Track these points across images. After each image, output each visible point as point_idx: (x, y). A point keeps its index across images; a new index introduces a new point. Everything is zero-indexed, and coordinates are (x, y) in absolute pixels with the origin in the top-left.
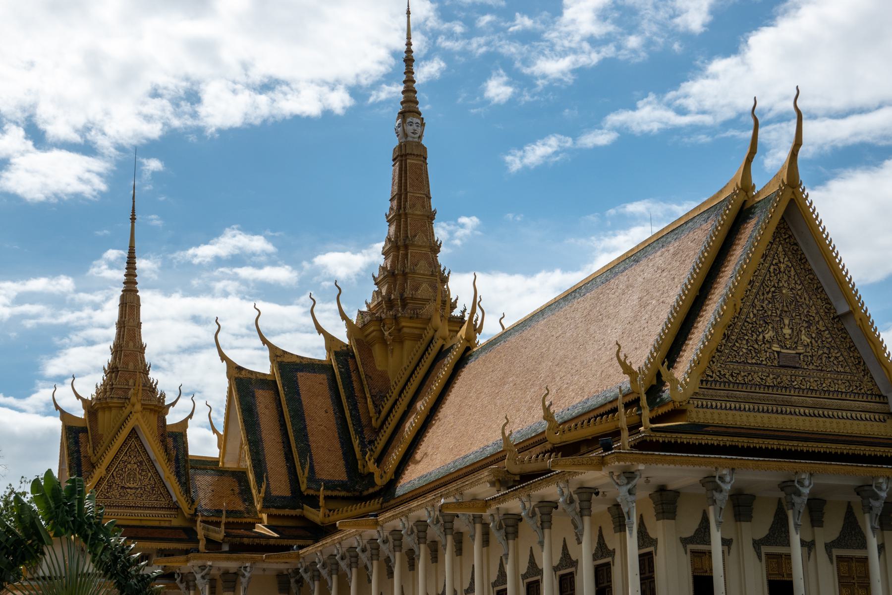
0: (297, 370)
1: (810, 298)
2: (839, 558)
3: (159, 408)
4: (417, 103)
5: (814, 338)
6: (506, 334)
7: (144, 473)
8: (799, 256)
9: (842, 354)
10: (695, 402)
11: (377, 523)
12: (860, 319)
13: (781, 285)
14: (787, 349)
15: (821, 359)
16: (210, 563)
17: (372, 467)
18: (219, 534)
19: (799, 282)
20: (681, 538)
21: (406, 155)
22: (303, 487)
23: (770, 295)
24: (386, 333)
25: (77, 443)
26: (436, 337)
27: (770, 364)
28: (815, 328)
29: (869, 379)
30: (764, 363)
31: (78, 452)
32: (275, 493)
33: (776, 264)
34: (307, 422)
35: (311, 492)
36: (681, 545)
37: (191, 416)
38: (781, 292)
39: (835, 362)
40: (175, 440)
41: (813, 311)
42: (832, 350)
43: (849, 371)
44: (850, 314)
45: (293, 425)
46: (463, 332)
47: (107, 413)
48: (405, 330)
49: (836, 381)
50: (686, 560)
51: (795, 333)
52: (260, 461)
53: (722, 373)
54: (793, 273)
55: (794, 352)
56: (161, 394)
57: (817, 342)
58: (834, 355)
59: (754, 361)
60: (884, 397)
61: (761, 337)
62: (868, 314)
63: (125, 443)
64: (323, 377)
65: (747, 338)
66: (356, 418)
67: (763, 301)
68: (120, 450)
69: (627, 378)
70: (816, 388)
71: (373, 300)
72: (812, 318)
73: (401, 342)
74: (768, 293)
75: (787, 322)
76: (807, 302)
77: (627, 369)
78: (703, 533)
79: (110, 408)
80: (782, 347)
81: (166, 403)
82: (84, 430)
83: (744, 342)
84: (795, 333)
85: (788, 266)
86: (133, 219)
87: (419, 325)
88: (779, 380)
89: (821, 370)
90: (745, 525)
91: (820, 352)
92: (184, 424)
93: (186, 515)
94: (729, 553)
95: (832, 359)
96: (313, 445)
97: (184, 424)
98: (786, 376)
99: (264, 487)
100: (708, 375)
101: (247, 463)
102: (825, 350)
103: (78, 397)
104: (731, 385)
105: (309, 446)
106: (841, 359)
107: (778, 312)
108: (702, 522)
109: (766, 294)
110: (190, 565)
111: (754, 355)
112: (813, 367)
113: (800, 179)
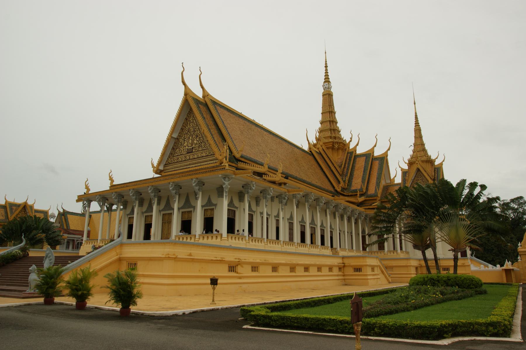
4: (329, 79)
5: (198, 141)
9: (206, 144)
13: (191, 127)
19: (196, 124)
42: (203, 143)
55: (192, 147)
57: (198, 142)
59: (180, 154)
74: (187, 131)
75: (191, 138)
85: (193, 120)
91: (199, 144)
107: (189, 136)
112: (197, 150)
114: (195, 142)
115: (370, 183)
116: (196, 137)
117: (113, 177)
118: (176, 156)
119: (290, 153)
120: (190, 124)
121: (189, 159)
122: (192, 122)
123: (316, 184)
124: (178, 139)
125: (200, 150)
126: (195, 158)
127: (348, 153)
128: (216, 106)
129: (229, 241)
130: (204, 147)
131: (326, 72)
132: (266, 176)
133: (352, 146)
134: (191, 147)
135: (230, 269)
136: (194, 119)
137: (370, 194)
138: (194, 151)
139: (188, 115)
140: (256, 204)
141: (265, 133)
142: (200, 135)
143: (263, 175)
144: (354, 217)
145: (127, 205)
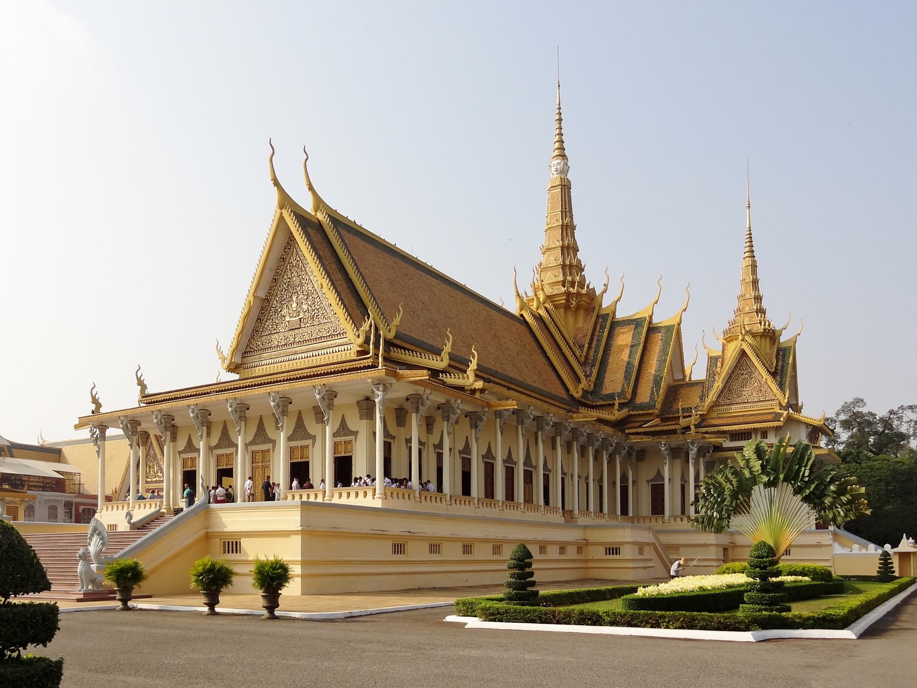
13: (293, 275)
28: (311, 298)
30: (281, 331)
42: (320, 310)
55: (298, 318)
57: (311, 307)
58: (321, 312)
59: (275, 331)
61: (280, 314)
65: (272, 318)
70: (309, 339)
74: (285, 284)
83: (271, 321)
84: (299, 305)
91: (313, 313)
95: (319, 316)
102: (316, 311)
107: (290, 295)
109: (284, 286)
112: (309, 325)
114: (305, 307)
115: (640, 379)
116: (306, 297)
117: (144, 380)
119: (482, 321)
120: (291, 270)
122: (294, 265)
123: (533, 384)
124: (268, 300)
125: (315, 324)
127: (598, 317)
128: (340, 229)
129: (423, 503)
130: (322, 317)
132: (446, 375)
133: (606, 303)
134: (295, 317)
135: (395, 549)
136: (299, 259)
137: (640, 404)
138: (303, 325)
139: (286, 250)
140: (426, 430)
141: (435, 282)
143: (440, 374)
144: (607, 450)
145: (176, 434)
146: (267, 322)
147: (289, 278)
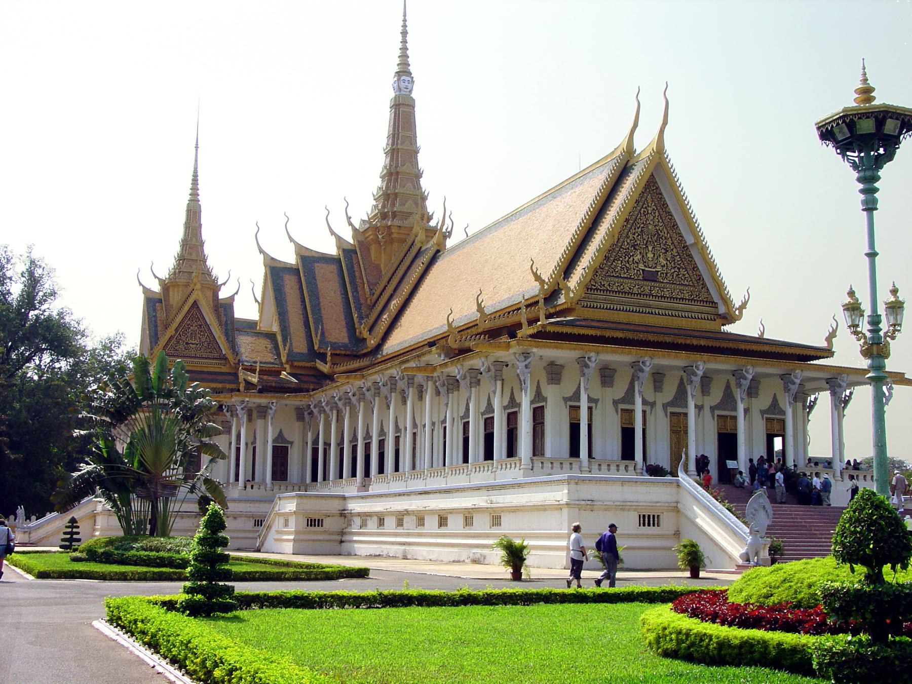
0: (314, 262)
1: (668, 233)
2: (672, 413)
3: (215, 288)
6: (470, 240)
7: (202, 333)
8: (662, 203)
10: (582, 303)
11: (363, 376)
12: (702, 249)
13: (648, 222)
14: (649, 268)
15: (673, 276)
16: (247, 399)
17: (366, 334)
18: (254, 379)
19: (661, 221)
20: (563, 397)
21: (399, 105)
22: (316, 347)
23: (640, 230)
24: (380, 237)
25: (154, 310)
26: (416, 241)
27: (636, 278)
29: (706, 291)
31: (155, 316)
32: (295, 350)
33: (646, 208)
34: (321, 300)
35: (322, 351)
36: (563, 402)
37: (237, 293)
38: (648, 227)
39: (683, 278)
40: (225, 310)
41: (670, 241)
43: (691, 284)
44: (695, 244)
45: (310, 301)
46: (435, 240)
47: (176, 290)
48: (395, 236)
49: (682, 291)
50: (566, 412)
51: (656, 257)
52: (285, 327)
53: (603, 283)
54: (657, 214)
55: (654, 270)
56: (215, 277)
57: (671, 263)
58: (682, 273)
59: (625, 276)
60: (715, 303)
61: (632, 259)
62: (707, 246)
63: (189, 311)
64: (334, 268)
65: (621, 259)
66: (357, 299)
67: (634, 234)
68: (185, 316)
69: (537, 284)
71: (372, 211)
72: (668, 247)
73: (391, 243)
74: (638, 228)
75: (650, 248)
76: (666, 235)
77: (537, 278)
78: (576, 396)
79: (178, 285)
80: (645, 266)
81: (219, 283)
82: (160, 301)
83: (619, 262)
84: (656, 257)
85: (654, 209)
86: (197, 147)
87: (405, 232)
88: (642, 289)
89: (673, 283)
90: (609, 390)
91: (673, 271)
92: (232, 298)
93: (232, 364)
94: (596, 407)
96: (324, 316)
97: (232, 298)
98: (647, 287)
99: (288, 345)
100: (592, 285)
101: (275, 328)
102: (676, 269)
103: (156, 277)
104: (608, 292)
105: (322, 317)
106: (687, 275)
107: (645, 242)
108: (577, 389)
110: (235, 400)
111: (626, 271)
113: (666, 148)
118: (613, 276)
120: (645, 216)
121: (651, 295)
126: (665, 297)
131: (404, 49)
142: (672, 250)
146: (614, 261)
147: (643, 223)
